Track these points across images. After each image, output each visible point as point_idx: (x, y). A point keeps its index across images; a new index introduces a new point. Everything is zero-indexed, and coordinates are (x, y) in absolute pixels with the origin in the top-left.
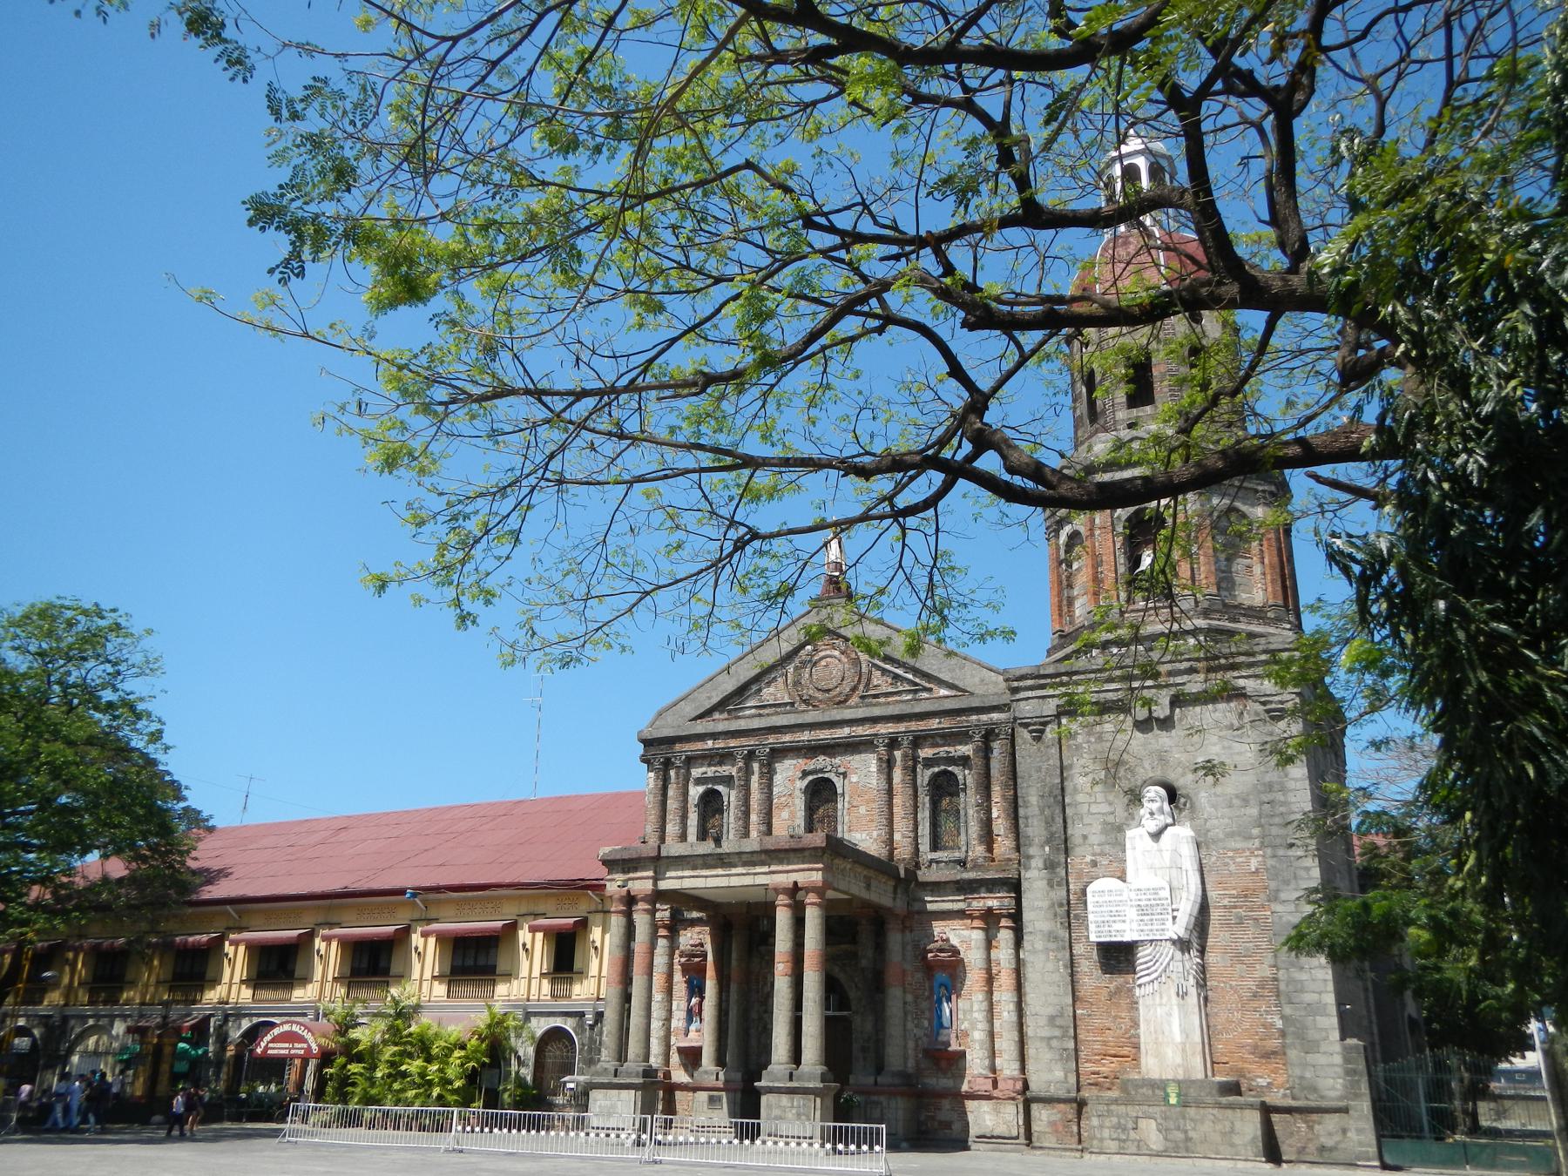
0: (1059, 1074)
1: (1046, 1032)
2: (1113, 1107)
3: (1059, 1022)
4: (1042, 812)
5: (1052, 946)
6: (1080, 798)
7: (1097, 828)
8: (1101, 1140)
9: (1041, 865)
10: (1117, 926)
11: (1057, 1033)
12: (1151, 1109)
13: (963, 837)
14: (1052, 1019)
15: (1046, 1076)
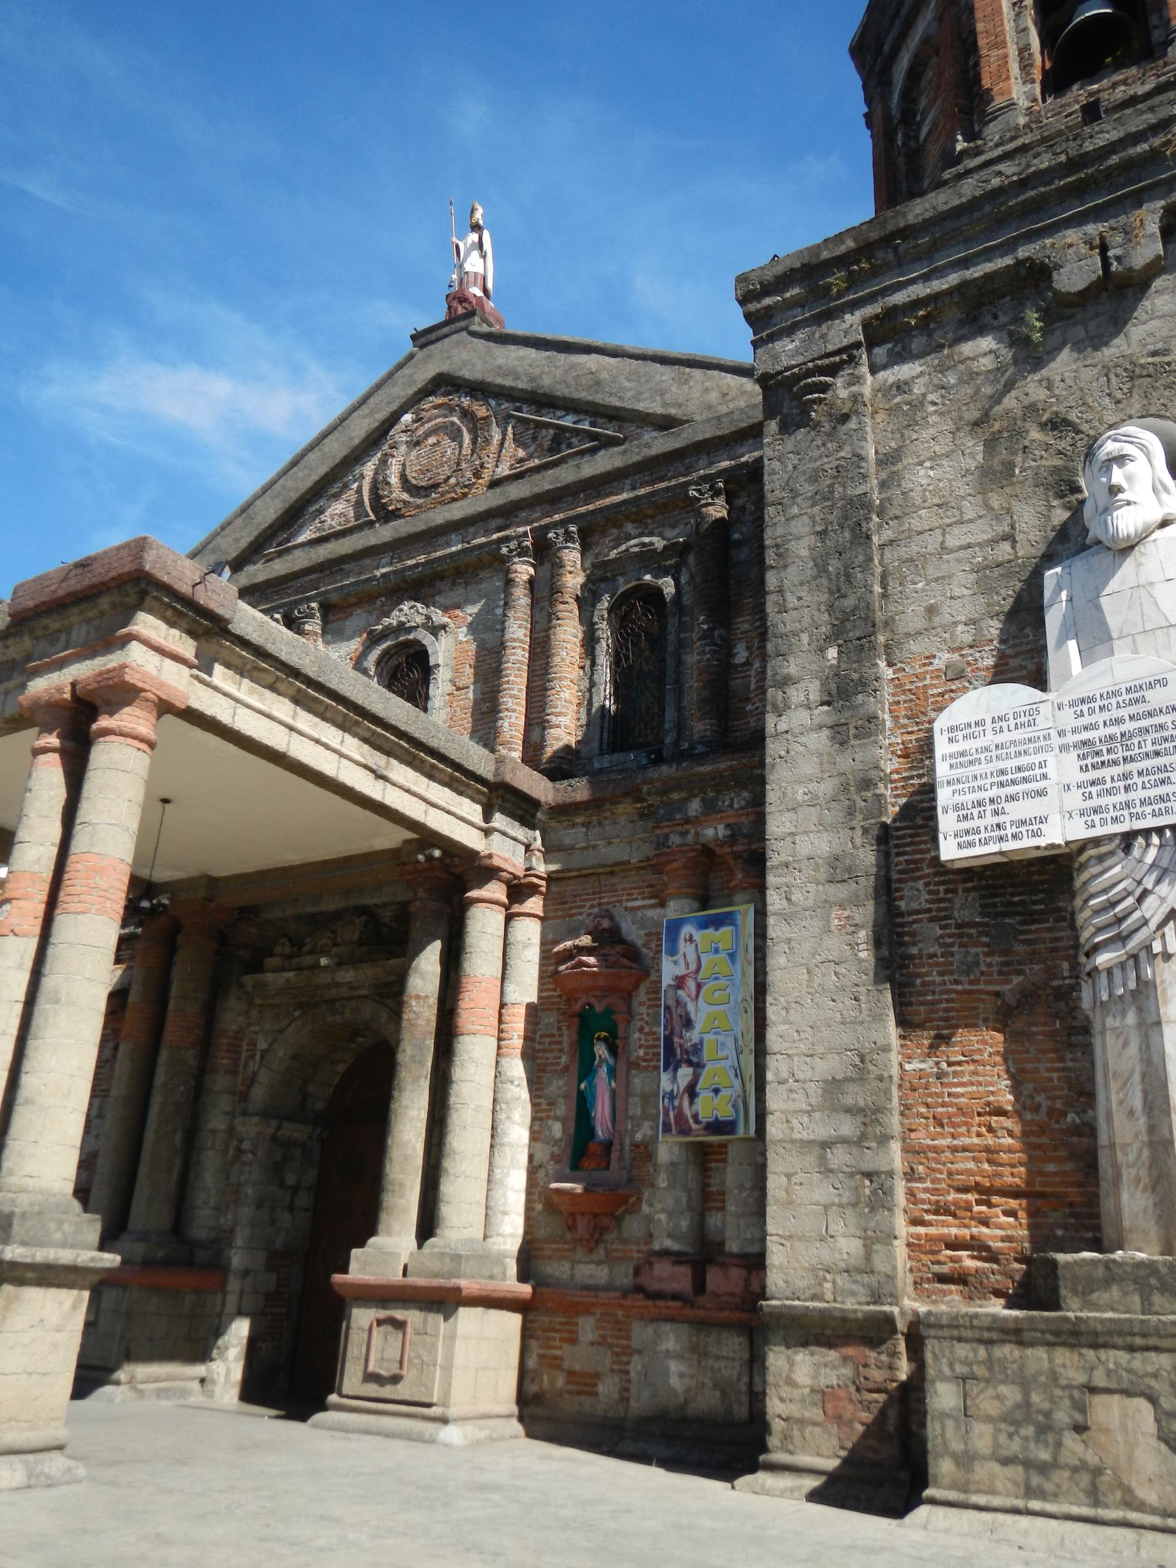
0: (849, 1247)
1: (821, 1129)
2: (1008, 1351)
3: (855, 1096)
4: (821, 569)
5: (842, 892)
6: (922, 519)
7: (962, 583)
8: (966, 1460)
9: (815, 696)
10: (1016, 811)
11: (847, 1127)
12: (1138, 1362)
13: (670, 714)
14: (833, 1086)
15: (812, 1254)
